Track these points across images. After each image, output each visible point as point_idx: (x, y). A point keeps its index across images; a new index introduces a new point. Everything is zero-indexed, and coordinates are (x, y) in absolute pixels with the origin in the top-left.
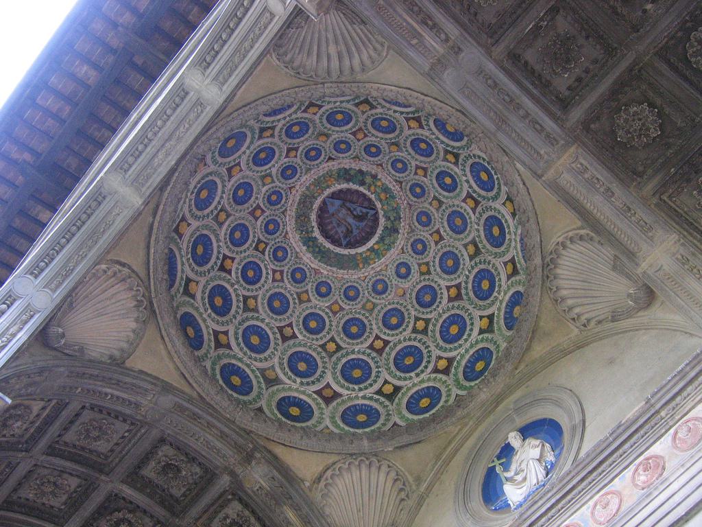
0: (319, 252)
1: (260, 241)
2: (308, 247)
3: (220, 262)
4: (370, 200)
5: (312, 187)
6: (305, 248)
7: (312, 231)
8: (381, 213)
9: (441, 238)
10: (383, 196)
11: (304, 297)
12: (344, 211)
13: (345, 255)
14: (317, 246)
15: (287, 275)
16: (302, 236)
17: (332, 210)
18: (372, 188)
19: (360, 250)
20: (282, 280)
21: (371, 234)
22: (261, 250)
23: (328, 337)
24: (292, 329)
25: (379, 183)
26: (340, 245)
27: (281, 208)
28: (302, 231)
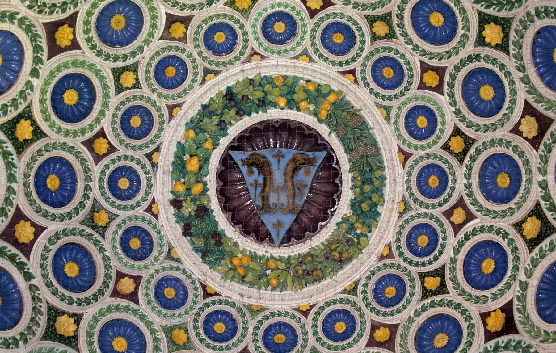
0: (371, 182)
1: (426, 293)
2: (375, 205)
3: (500, 339)
4: (221, 176)
5: (274, 282)
6: (380, 209)
7: (345, 220)
8: (224, 142)
9: (171, 20)
10: (193, 165)
11: (457, 145)
12: (273, 199)
13: (338, 135)
14: (362, 193)
15: (445, 201)
16: (365, 230)
17: (288, 220)
18: (197, 189)
19: (310, 120)
20: (460, 203)
22: (438, 279)
23: (483, 51)
24: (519, 123)
25: (181, 189)
26: (330, 159)
27: (348, 301)
28: (358, 237)
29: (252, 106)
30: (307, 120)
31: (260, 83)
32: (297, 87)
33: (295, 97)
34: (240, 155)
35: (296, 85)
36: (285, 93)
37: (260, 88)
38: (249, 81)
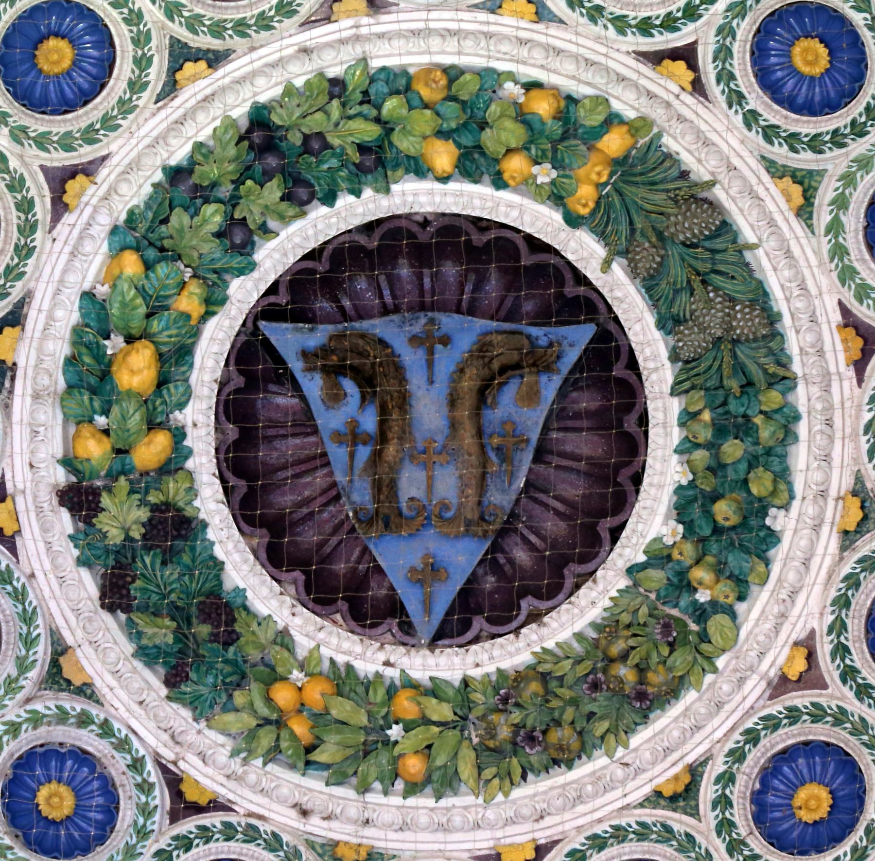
21: (356, 250)
29: (339, 169)
30: (527, 218)
31: (365, 93)
32: (493, 107)
33: (487, 137)
34: (299, 335)
35: (491, 100)
36: (453, 125)
37: (365, 108)
38: (326, 84)
